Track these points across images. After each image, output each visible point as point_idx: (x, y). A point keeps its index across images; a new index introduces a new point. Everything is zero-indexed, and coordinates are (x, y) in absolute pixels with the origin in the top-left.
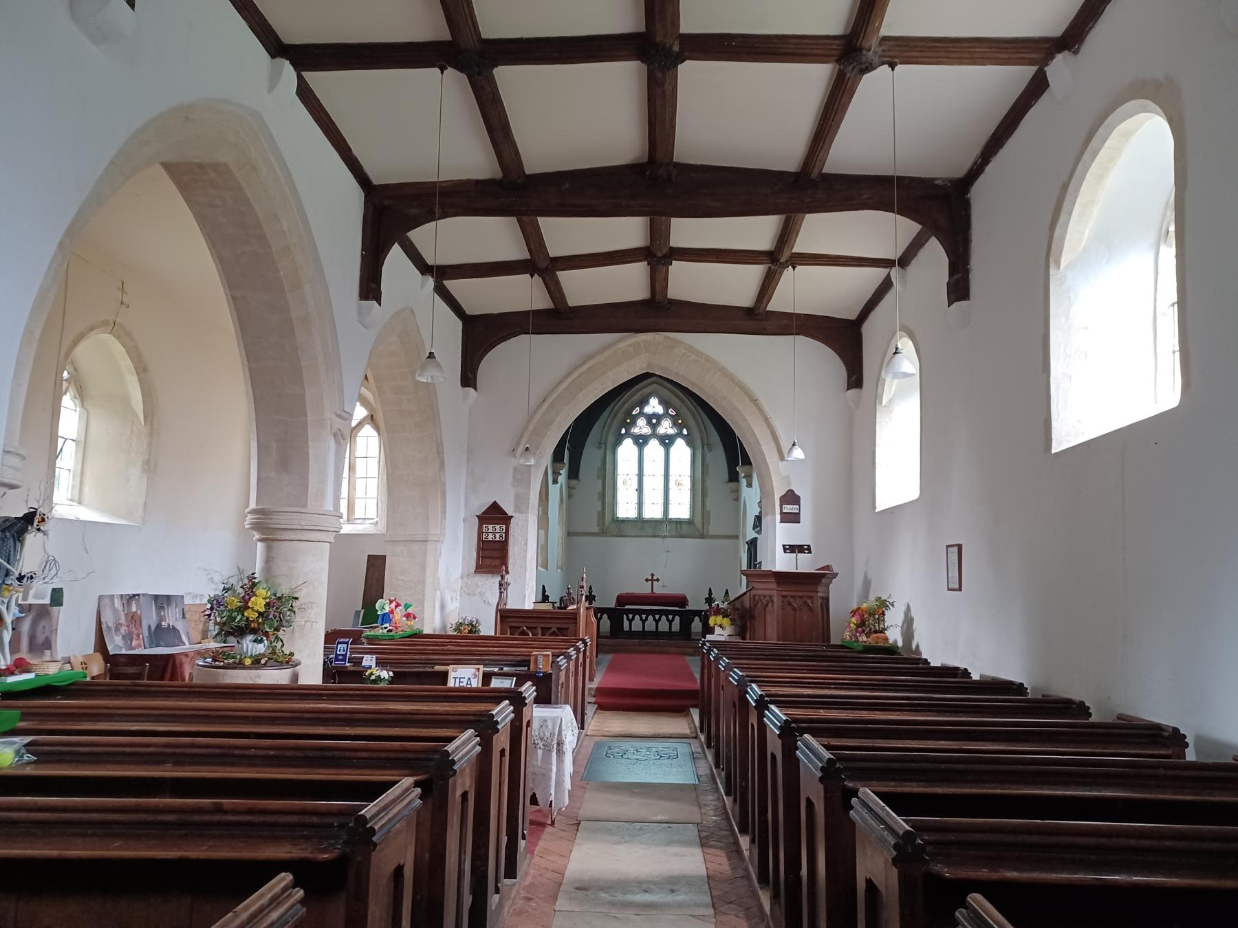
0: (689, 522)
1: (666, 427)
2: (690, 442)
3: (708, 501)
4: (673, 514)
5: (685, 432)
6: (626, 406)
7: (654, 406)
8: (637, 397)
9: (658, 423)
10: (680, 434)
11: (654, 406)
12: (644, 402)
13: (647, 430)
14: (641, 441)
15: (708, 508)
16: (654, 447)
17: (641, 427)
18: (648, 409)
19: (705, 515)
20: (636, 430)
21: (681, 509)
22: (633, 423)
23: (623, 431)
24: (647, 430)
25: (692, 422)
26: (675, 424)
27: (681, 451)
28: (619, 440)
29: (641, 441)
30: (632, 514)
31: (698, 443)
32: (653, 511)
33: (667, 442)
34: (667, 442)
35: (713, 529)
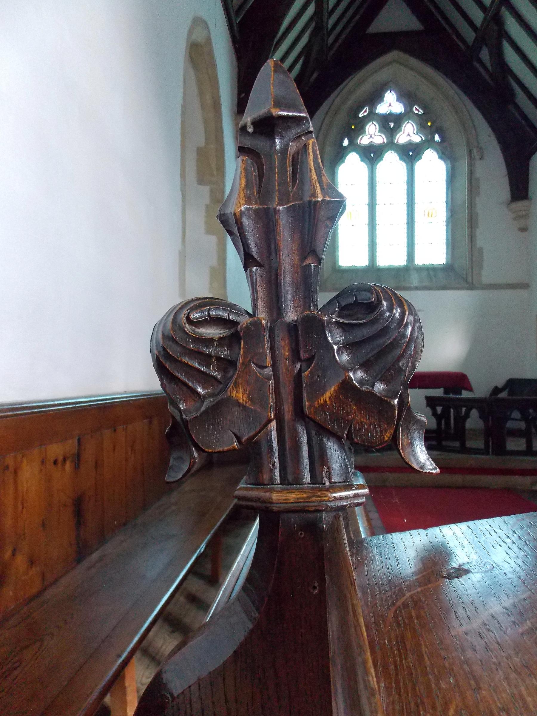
0: (448, 268)
1: (409, 133)
2: (446, 153)
3: (478, 232)
4: (420, 260)
5: (437, 138)
6: (350, 103)
7: (391, 103)
8: (366, 87)
9: (398, 127)
10: (428, 143)
11: (391, 103)
12: (376, 97)
13: (379, 139)
14: (372, 155)
15: (479, 243)
16: (391, 164)
17: (372, 135)
18: (382, 109)
19: (475, 256)
20: (364, 140)
21: (433, 251)
22: (360, 129)
23: (346, 142)
24: (379, 139)
25: (449, 120)
26: (422, 127)
27: (432, 167)
28: (339, 155)
29: (372, 155)
30: (362, 261)
31: (462, 152)
32: (391, 257)
33: (410, 154)
34: (410, 154)
35: (487, 275)
